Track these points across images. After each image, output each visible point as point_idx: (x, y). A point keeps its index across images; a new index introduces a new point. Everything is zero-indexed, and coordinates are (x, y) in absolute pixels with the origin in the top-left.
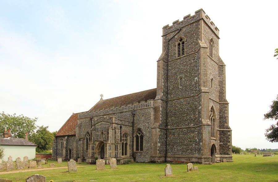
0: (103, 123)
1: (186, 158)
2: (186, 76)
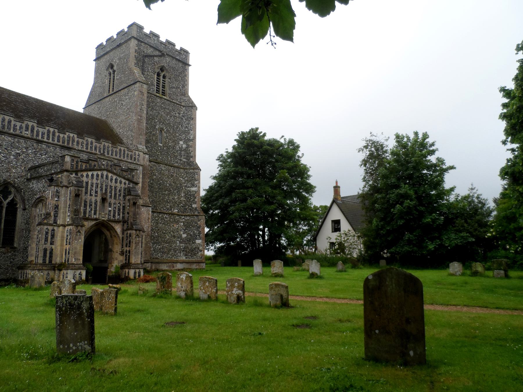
0: (107, 176)
1: (167, 264)
2: (167, 130)
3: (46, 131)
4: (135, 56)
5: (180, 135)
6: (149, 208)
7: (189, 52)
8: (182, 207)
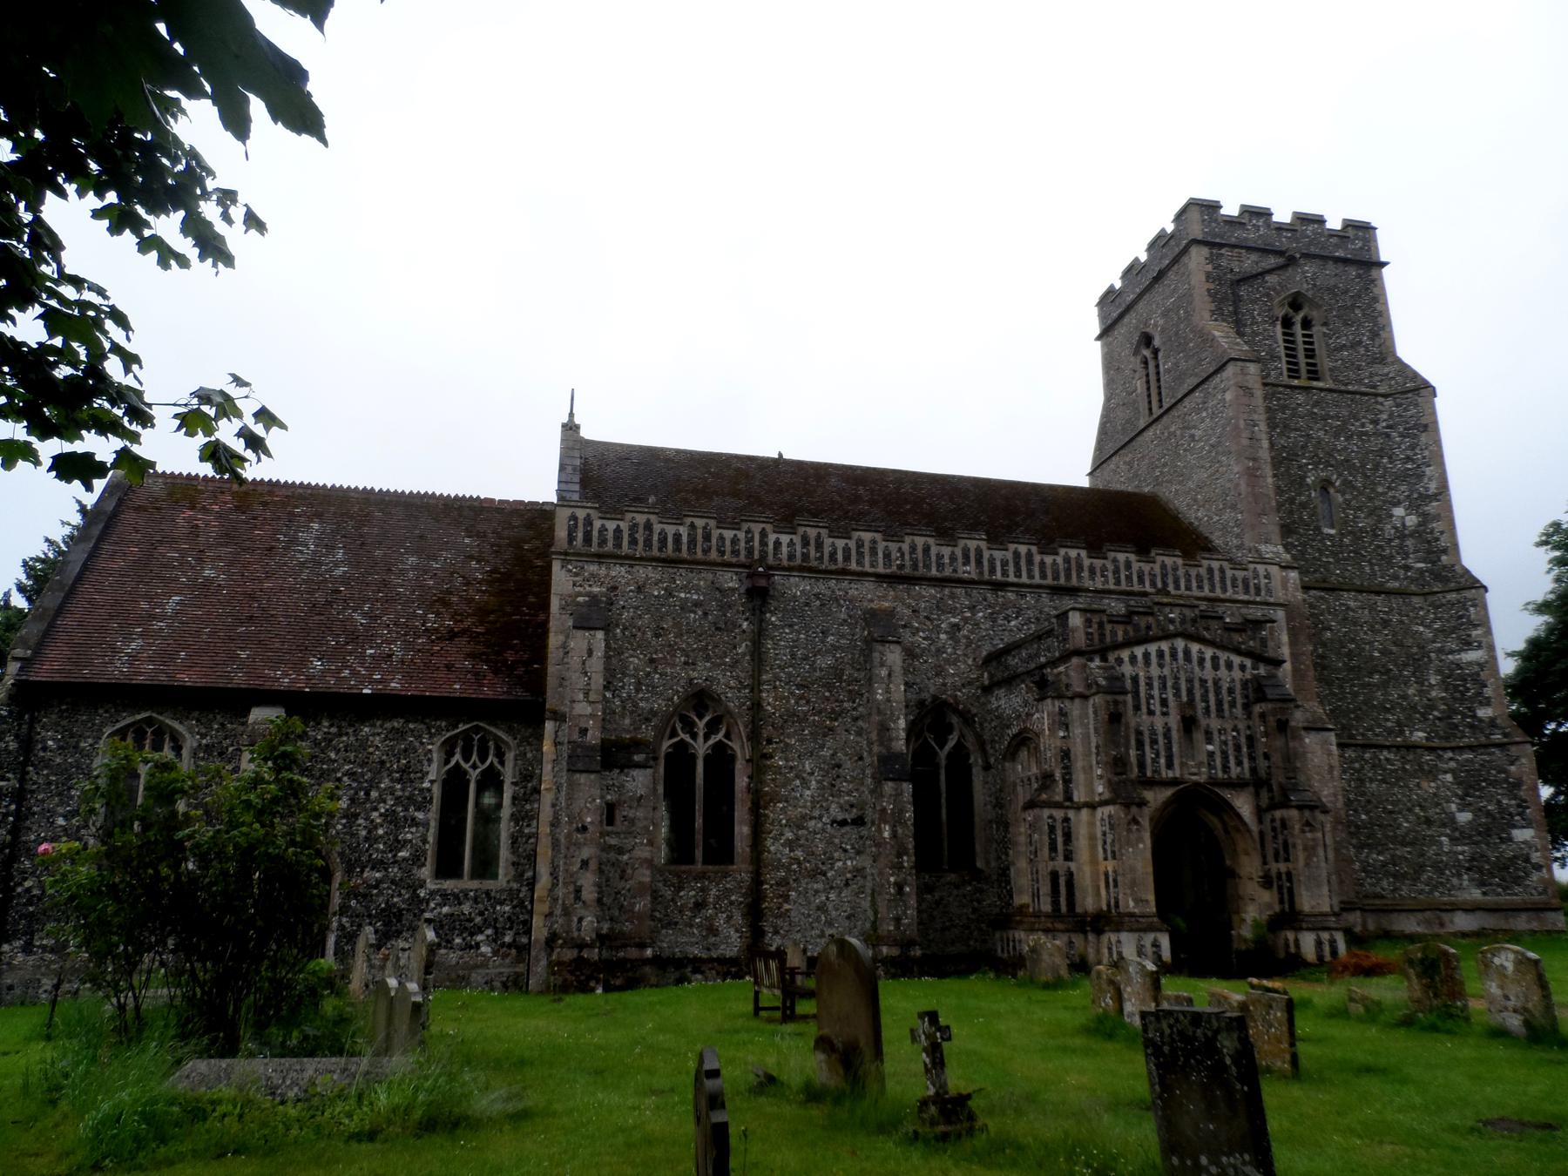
0: (1187, 652)
1: (1419, 915)
2: (1346, 483)
3: (1009, 555)
4: (1208, 290)
5: (1389, 488)
6: (1326, 734)
7: (1373, 224)
8: (1439, 719)
